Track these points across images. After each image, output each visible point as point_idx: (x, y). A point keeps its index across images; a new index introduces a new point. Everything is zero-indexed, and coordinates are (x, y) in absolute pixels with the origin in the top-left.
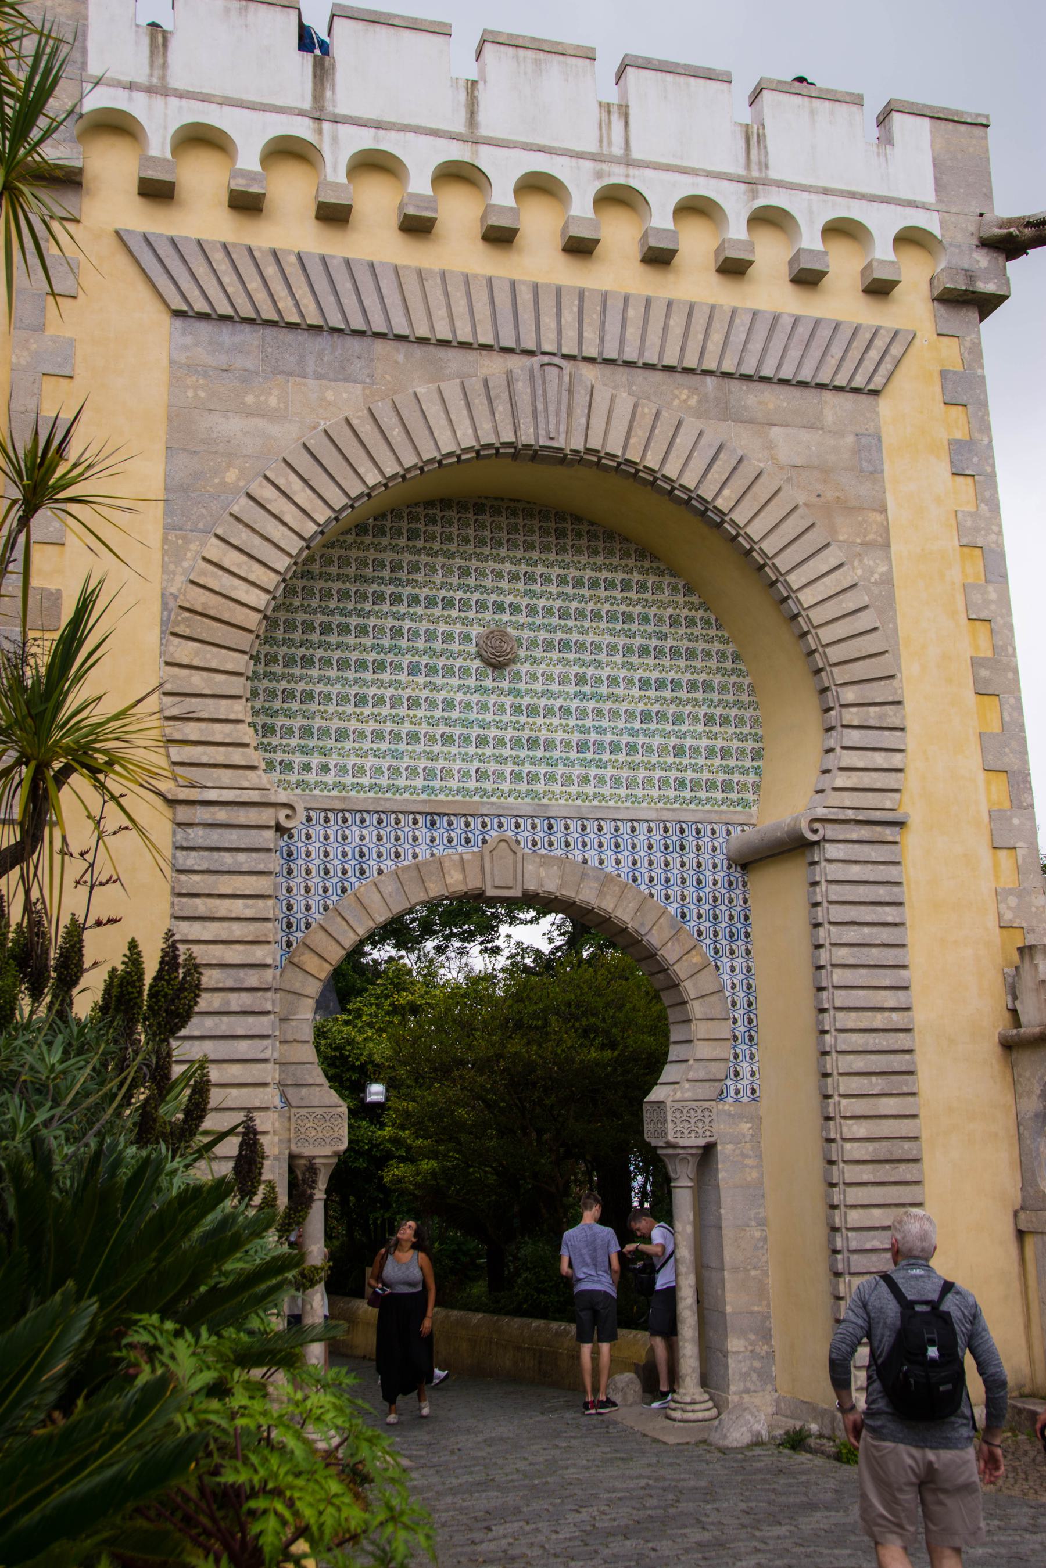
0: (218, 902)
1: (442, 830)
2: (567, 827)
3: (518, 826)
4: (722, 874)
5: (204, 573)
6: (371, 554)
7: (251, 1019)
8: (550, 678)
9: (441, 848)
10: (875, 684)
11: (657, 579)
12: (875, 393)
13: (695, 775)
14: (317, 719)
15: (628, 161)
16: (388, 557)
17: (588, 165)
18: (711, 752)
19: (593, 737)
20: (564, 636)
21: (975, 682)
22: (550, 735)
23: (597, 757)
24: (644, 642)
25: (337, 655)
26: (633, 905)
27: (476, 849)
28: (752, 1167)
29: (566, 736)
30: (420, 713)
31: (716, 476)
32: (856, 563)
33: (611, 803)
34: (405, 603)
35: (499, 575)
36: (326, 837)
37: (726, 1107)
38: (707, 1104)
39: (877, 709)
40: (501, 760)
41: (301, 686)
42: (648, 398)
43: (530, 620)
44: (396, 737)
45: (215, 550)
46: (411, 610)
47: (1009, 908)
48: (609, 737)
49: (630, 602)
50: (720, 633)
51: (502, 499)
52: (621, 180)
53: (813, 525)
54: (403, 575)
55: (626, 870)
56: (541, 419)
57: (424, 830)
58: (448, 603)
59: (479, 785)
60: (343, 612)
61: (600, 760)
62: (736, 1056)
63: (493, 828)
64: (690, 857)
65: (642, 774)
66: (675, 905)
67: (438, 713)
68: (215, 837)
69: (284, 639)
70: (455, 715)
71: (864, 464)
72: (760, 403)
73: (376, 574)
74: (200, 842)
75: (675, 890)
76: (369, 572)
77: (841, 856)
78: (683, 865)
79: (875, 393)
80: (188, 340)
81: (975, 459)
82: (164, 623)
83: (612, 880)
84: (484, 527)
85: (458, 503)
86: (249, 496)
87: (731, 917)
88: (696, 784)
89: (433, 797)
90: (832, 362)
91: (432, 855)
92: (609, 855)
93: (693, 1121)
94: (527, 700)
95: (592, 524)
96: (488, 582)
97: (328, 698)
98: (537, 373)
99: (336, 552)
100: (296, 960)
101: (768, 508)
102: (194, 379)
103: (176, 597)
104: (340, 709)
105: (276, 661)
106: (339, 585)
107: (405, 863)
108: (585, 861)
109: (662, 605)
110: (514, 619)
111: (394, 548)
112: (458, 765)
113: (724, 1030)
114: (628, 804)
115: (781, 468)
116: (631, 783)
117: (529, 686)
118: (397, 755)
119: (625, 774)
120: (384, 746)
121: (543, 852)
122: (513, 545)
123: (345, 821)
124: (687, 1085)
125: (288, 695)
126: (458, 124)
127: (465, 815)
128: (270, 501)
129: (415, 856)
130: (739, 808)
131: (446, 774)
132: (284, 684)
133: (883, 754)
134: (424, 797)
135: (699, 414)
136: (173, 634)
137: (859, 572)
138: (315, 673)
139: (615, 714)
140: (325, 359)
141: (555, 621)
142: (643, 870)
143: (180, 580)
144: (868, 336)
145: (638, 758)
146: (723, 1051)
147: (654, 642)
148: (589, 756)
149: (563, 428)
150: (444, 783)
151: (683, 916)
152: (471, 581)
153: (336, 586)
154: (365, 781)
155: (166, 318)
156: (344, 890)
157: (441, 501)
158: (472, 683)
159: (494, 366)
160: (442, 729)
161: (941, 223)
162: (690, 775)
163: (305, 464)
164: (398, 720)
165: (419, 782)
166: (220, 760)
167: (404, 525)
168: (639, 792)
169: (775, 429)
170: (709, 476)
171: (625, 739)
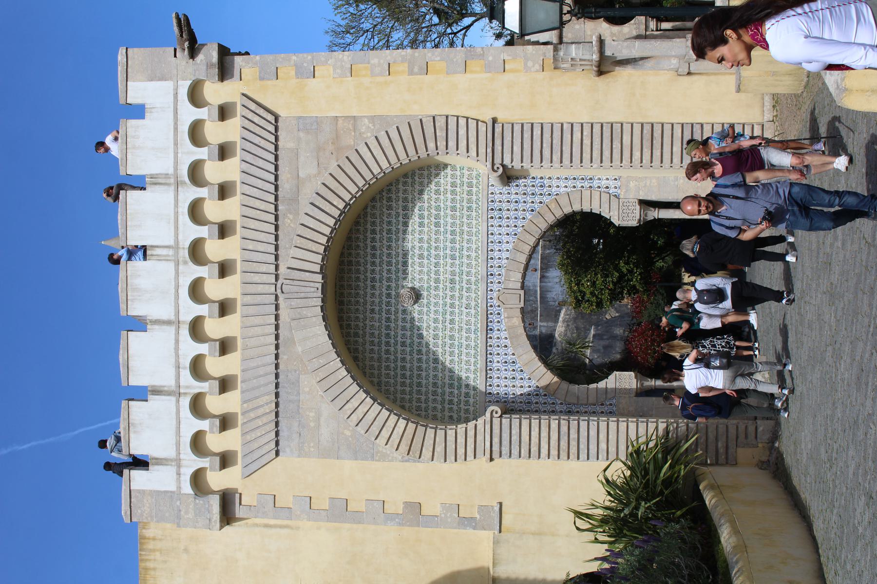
0: (532, 442)
1: (494, 325)
2: (492, 267)
3: (491, 290)
4: (512, 189)
5: (392, 446)
6: (367, 355)
7: (581, 429)
9: (502, 326)
10: (426, 132)
11: (369, 216)
12: (276, 120)
13: (465, 201)
14: (445, 381)
15: (176, 247)
17: (181, 267)
18: (453, 193)
19: (448, 252)
21: (421, 74)
22: (449, 273)
23: (458, 250)
24: (401, 224)
25: (415, 372)
26: (528, 236)
27: (502, 310)
28: (651, 182)
30: (441, 334)
31: (328, 208)
32: (365, 136)
33: (480, 244)
35: (373, 294)
36: (498, 378)
37: (622, 193)
38: (621, 204)
39: (437, 131)
41: (430, 388)
42: (292, 239)
43: (394, 281)
44: (452, 345)
45: (382, 440)
47: (533, 66)
48: (448, 244)
49: (381, 231)
51: (336, 292)
52: (187, 251)
53: (347, 158)
54: (376, 340)
56: (309, 295)
58: (388, 320)
59: (473, 308)
60: (395, 369)
61: (459, 249)
62: (599, 187)
63: (493, 302)
64: (505, 206)
65: (465, 228)
67: (440, 326)
68: (505, 442)
69: (409, 395)
70: (441, 318)
73: (376, 353)
74: (508, 449)
76: (376, 356)
78: (508, 210)
79: (276, 120)
80: (288, 450)
81: (305, 65)
82: (415, 461)
84: (350, 301)
85: (339, 313)
86: (357, 426)
87: (533, 186)
90: (263, 143)
91: (505, 330)
92: (504, 246)
93: (628, 211)
94: (432, 283)
95: (344, 247)
96: (377, 300)
97: (435, 376)
99: (367, 370)
100: (552, 393)
103: (403, 457)
104: (440, 371)
105: (419, 399)
106: (383, 369)
108: (507, 258)
109: (382, 214)
110: (394, 289)
112: (464, 317)
113: (586, 193)
114: (480, 236)
115: (319, 173)
116: (470, 234)
117: (426, 282)
119: (466, 237)
120: (457, 351)
121: (503, 278)
123: (491, 370)
124: (611, 213)
125: (435, 393)
126: (172, 330)
127: (487, 315)
128: (358, 418)
129: (506, 338)
130: (480, 179)
131: (468, 323)
133: (459, 130)
134: (479, 334)
136: (420, 457)
137: (369, 135)
138: (424, 382)
139: (437, 240)
140: (290, 391)
141: (393, 268)
143: (395, 454)
144: (247, 121)
145: (458, 230)
146: (596, 196)
147: (400, 219)
148: (457, 254)
149: (312, 284)
150: (473, 324)
152: (377, 308)
153: (383, 372)
154: (473, 360)
156: (522, 371)
157: (339, 321)
158: (425, 309)
159: (282, 312)
160: (447, 324)
161: (183, 80)
163: (340, 402)
165: (473, 336)
167: (352, 339)
168: (474, 230)
170: (328, 211)
171: (449, 236)
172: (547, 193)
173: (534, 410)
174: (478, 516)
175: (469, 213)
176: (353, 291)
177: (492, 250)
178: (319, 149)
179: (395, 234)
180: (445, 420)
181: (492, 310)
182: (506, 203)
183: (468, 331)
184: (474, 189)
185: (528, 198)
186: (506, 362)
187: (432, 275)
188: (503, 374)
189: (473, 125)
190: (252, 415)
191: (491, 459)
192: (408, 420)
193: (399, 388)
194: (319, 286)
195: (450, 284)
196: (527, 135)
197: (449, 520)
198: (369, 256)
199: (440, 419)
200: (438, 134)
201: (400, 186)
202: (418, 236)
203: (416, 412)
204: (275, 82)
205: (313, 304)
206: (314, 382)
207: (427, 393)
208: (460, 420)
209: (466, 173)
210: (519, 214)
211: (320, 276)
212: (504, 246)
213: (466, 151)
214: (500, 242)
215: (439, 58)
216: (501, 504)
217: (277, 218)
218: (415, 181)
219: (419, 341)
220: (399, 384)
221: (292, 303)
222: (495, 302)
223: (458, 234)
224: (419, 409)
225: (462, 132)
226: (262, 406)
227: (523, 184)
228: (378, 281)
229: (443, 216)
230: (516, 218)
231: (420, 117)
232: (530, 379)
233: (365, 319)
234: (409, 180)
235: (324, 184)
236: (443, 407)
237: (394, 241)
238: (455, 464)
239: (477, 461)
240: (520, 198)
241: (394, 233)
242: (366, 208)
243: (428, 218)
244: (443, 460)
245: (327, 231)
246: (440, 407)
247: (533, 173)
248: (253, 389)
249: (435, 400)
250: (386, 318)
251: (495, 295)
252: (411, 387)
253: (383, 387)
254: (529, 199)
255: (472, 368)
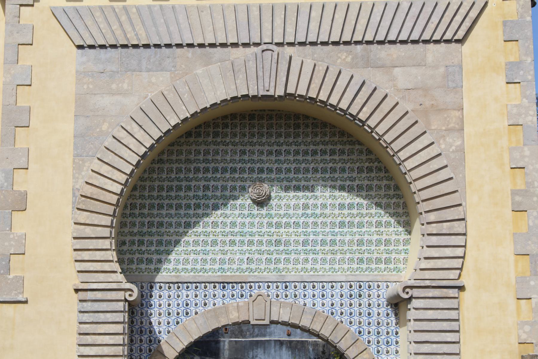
0: (97, 337)
1: (229, 291)
2: (295, 287)
3: (269, 287)
4: (383, 309)
5: (91, 177)
6: (194, 147)
8: (288, 206)
9: (228, 300)
10: (448, 210)
11: (351, 147)
12: (458, 41)
13: (369, 256)
16: (202, 148)
19: (312, 237)
20: (297, 183)
23: (313, 248)
24: (342, 183)
25: (175, 202)
26: (331, 327)
27: (246, 300)
29: (296, 238)
30: (218, 230)
31: (359, 101)
32: (441, 142)
33: (320, 273)
34: (211, 172)
35: (262, 153)
36: (169, 296)
39: (448, 224)
40: (260, 252)
41: (157, 219)
42: (323, 61)
43: (278, 176)
44: (205, 243)
46: (214, 176)
47: (524, 332)
48: (320, 237)
50: (387, 175)
51: (264, 110)
53: (416, 122)
54: (210, 157)
56: (260, 81)
57: (219, 291)
58: (234, 170)
59: (248, 266)
64: (365, 301)
65: (339, 256)
66: (355, 327)
67: (227, 230)
69: (149, 196)
70: (236, 230)
71: (450, 83)
72: (388, 55)
73: (196, 158)
75: (356, 318)
76: (192, 157)
77: (422, 306)
78: (360, 305)
80: (84, 59)
82: (73, 203)
83: (319, 314)
84: (254, 127)
86: (114, 137)
87: (388, 333)
88: (369, 260)
89: (224, 274)
91: (224, 304)
92: (319, 301)
94: (275, 220)
95: (315, 119)
96: (255, 157)
97: (171, 225)
98: (259, 55)
99: (176, 148)
101: (389, 116)
102: (87, 79)
103: (78, 190)
104: (177, 230)
107: (209, 308)
108: (305, 305)
109: (353, 162)
110: (269, 176)
111: (206, 143)
112: (238, 256)
115: (399, 90)
116: (332, 261)
117: (277, 212)
118: (206, 253)
119: (329, 256)
120: (199, 248)
121: (283, 300)
122: (270, 135)
123: (179, 287)
125: (151, 224)
127: (240, 283)
128: (123, 138)
130: (394, 273)
132: (148, 219)
133: (450, 249)
134: (219, 274)
135: (352, 66)
136: (78, 209)
137: (443, 146)
138: (164, 212)
139: (324, 224)
140: (152, 60)
141: (292, 175)
142: (337, 309)
143: (81, 183)
144: (456, 8)
145: (336, 248)
148: (309, 248)
149: (273, 84)
150: (230, 266)
152: (246, 157)
153: (175, 166)
155: (75, 49)
156: (178, 323)
157: (231, 114)
158: (246, 212)
160: (230, 237)
162: (366, 255)
163: (140, 117)
164: (207, 234)
165: (217, 266)
166: (99, 269)
167: (211, 130)
168: (337, 266)
169: (396, 69)
170: (355, 101)
171: (329, 238)
172: (380, 349)
173: (133, 338)
174: (11, 276)
175: (355, 260)
176: (265, 130)
177: (314, 287)
178: (426, 90)
179: (330, 177)
180: (120, 236)
181: (247, 289)
182: (367, 302)
183: (222, 261)
184: (383, 266)
185: (374, 327)
186: (187, 305)
187: (284, 220)
188: (174, 302)
189: (457, 263)
190: (123, 18)
191: (77, 291)
192: (121, 195)
193: (157, 183)
194: (271, 93)
195: (274, 239)
196: (445, 326)
197: (6, 244)
198: (305, 148)
199: (122, 230)
200: (445, 224)
201: (385, 182)
202: (329, 203)
203: (129, 203)
204: (501, 38)
205: (251, 86)
206: (162, 88)
207: (150, 215)
208: (121, 254)
209: (402, 256)
210: (356, 318)
211: (282, 93)
212: (319, 301)
213: (426, 256)
214: (323, 296)
215: (531, 224)
216: (26, 302)
217: (346, 43)
218: (391, 199)
219: (210, 206)
220: (160, 183)
221: (251, 62)
222: (255, 292)
223: (331, 248)
224: (133, 206)
225: (448, 252)
226: (134, 29)
227: (389, 321)
228: (277, 158)
229: (352, 231)
230: (351, 314)
231: (464, 204)
232: (168, 333)
233: (235, 144)
234: (392, 192)
235: (386, 96)
236: (135, 234)
237: (323, 176)
238: (70, 249)
239: (75, 274)
240: (375, 318)
241: (332, 176)
242: (360, 143)
243: (349, 214)
244: (75, 235)
245: (333, 101)
246: (135, 230)
247: (403, 331)
248: (153, 19)
249: (143, 224)
250: (236, 168)
251: (264, 291)
252: (158, 197)
253: (157, 166)
254: (373, 328)
255: (180, 267)
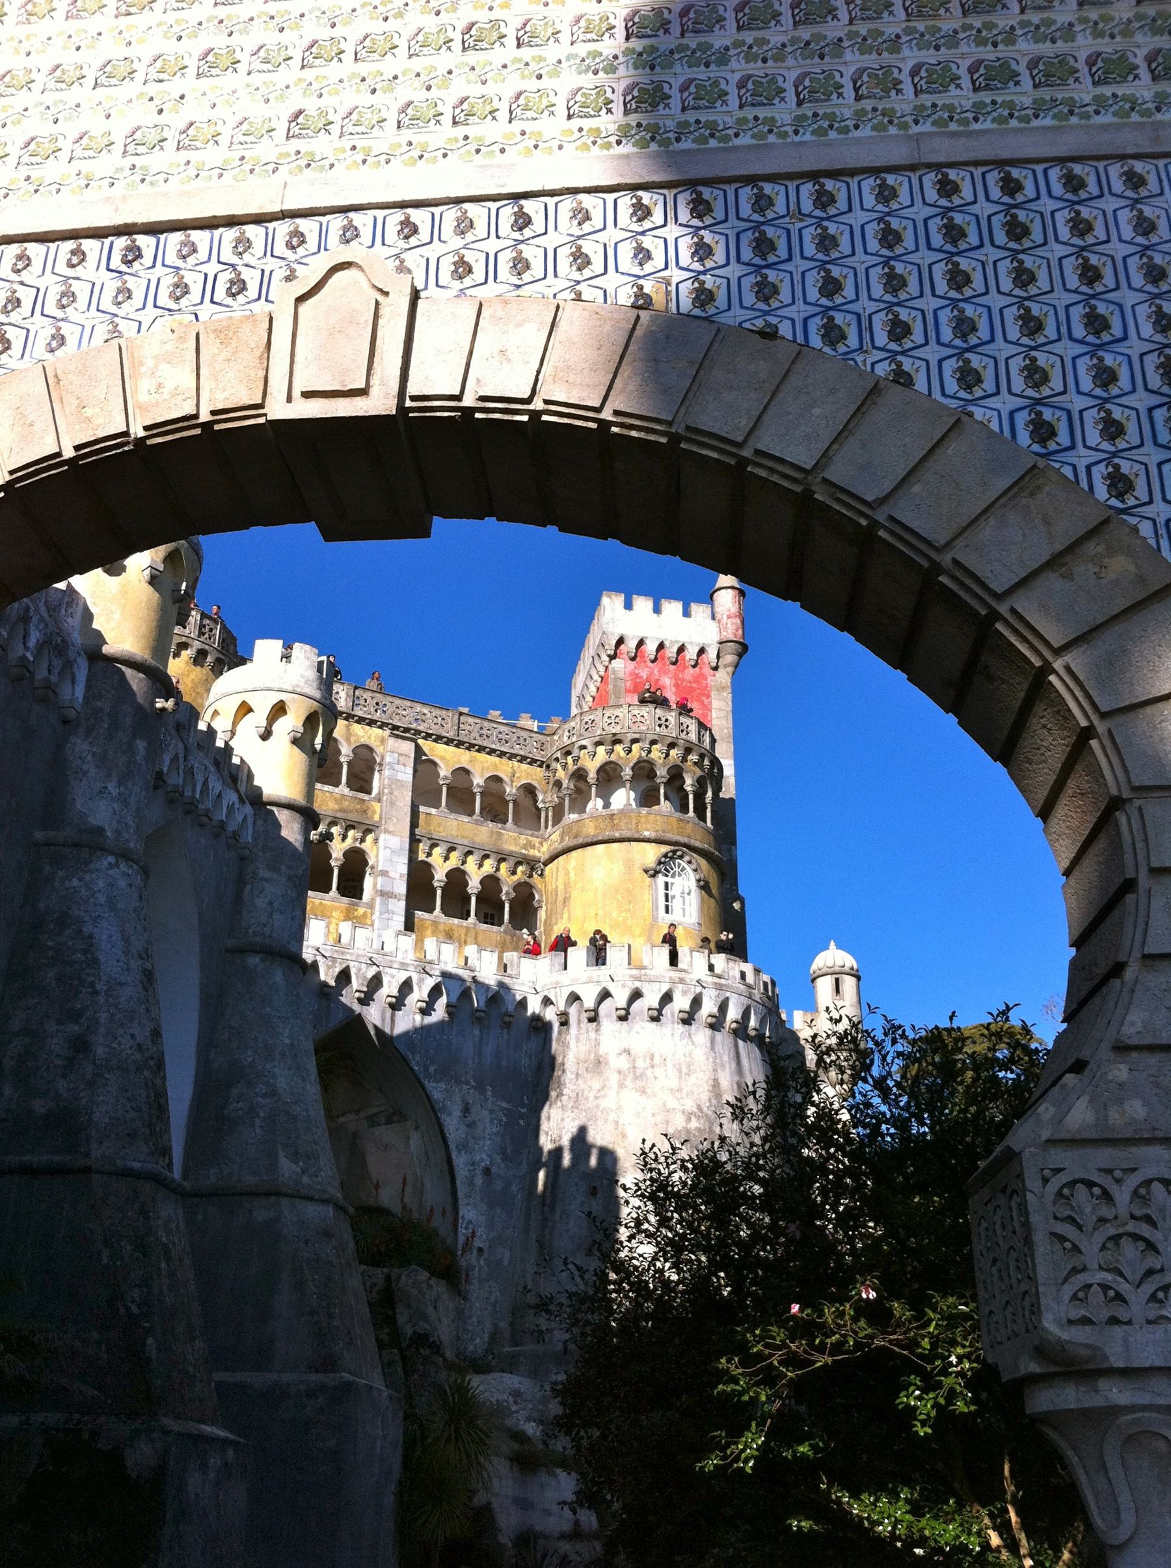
33: (745, 140)
55: (799, 311)
151: (1042, 431)
